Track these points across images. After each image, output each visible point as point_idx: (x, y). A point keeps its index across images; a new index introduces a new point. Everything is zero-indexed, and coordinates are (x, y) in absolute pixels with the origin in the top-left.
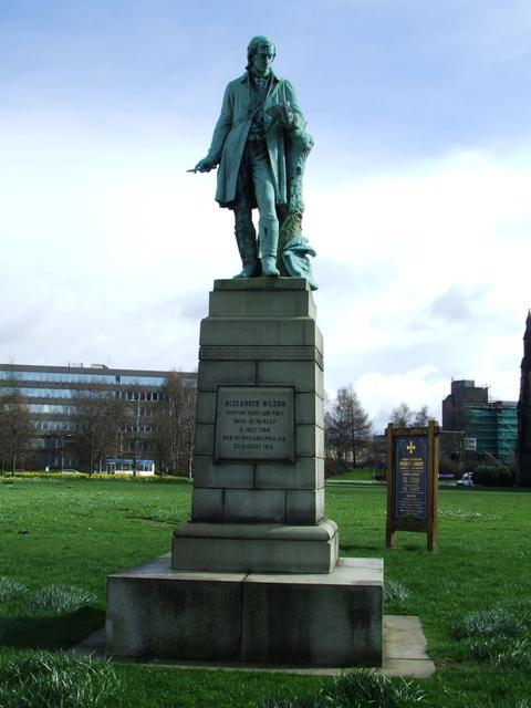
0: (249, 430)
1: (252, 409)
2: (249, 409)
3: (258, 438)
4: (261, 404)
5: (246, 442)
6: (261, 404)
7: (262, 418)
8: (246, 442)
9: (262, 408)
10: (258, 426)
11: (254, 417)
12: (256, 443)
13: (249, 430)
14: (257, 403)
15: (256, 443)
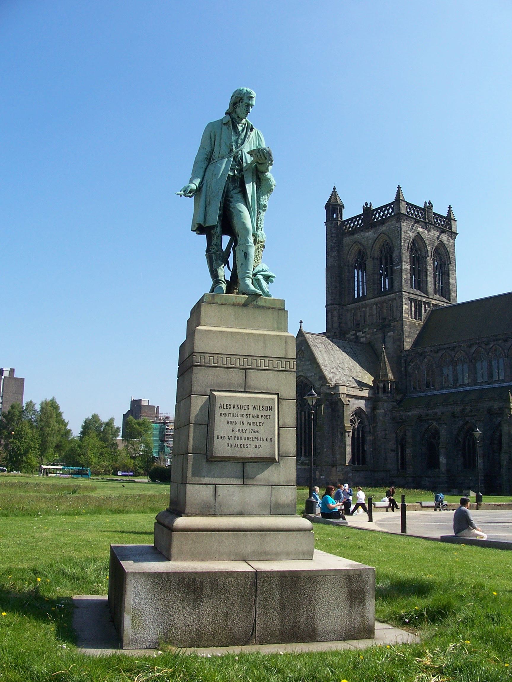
0: (240, 431)
1: (243, 412)
2: (240, 412)
3: (249, 439)
4: (251, 408)
5: (238, 442)
6: (251, 408)
7: (252, 420)
8: (238, 442)
9: (252, 412)
10: (249, 427)
11: (245, 420)
12: (248, 442)
13: (240, 431)
14: (248, 407)
15: (248, 442)
